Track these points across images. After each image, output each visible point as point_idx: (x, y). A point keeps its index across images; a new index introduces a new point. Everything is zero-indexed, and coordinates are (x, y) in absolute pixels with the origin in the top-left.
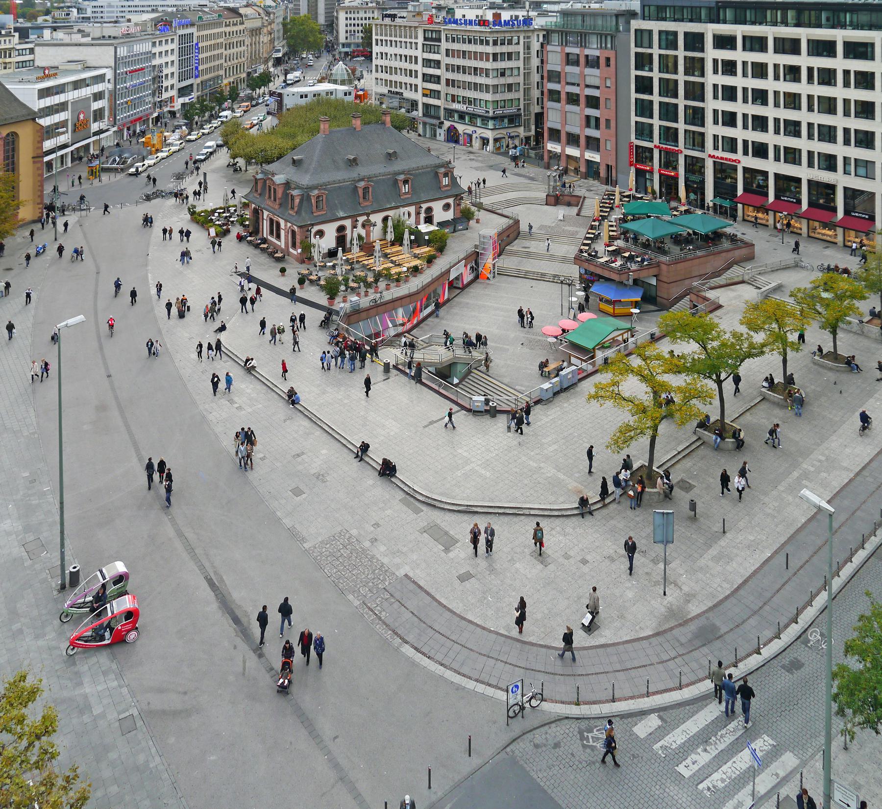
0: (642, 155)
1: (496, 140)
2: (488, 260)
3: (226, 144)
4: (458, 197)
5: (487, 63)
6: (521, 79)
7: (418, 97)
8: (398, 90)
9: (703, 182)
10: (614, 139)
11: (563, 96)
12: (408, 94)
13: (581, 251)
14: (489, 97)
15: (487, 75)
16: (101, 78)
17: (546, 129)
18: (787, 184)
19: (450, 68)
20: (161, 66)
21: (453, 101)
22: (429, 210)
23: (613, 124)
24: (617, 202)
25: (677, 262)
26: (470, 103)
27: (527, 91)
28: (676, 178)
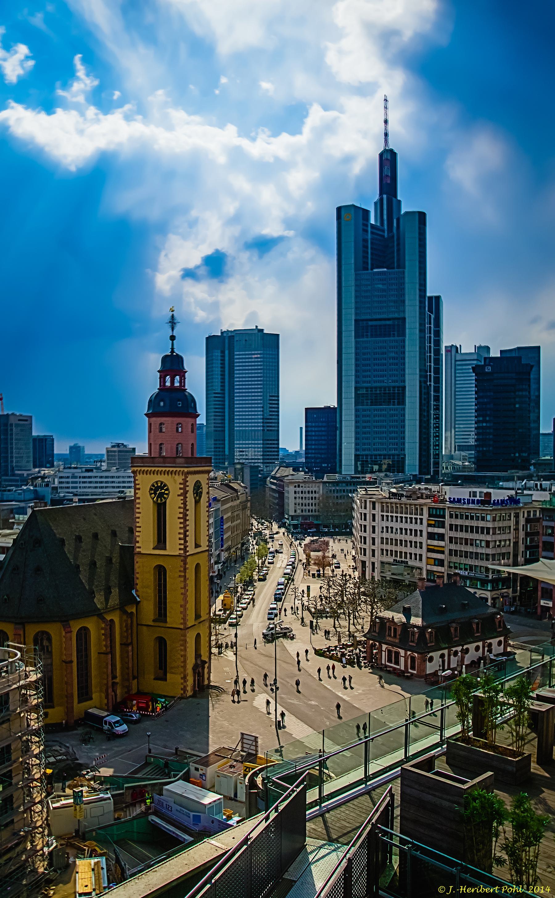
1: (493, 599)
5: (488, 536)
7: (423, 564)
8: (403, 559)
17: (540, 589)
21: (456, 568)
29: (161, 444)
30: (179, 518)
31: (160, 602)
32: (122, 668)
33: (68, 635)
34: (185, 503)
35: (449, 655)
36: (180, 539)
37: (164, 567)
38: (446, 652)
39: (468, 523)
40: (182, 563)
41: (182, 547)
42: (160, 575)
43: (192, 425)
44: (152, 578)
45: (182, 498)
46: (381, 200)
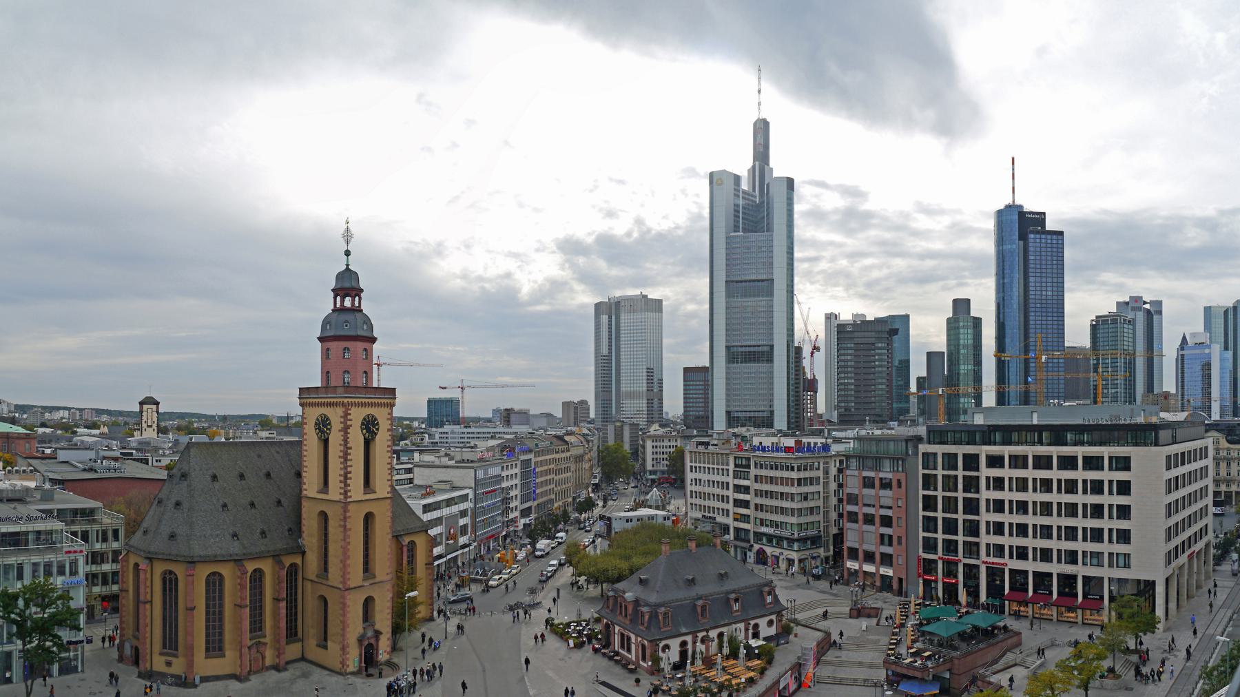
0: (929, 566)
2: (810, 669)
3: (569, 562)
4: (779, 614)
6: (820, 503)
7: (729, 521)
9: (978, 586)
11: (861, 517)
13: (888, 655)
14: (794, 520)
15: (792, 500)
16: (464, 498)
17: (845, 547)
18: (1042, 579)
19: (759, 493)
20: (507, 488)
21: (762, 525)
22: (756, 626)
23: (904, 540)
24: (912, 610)
25: (968, 654)
26: (777, 526)
27: (826, 513)
28: (956, 584)
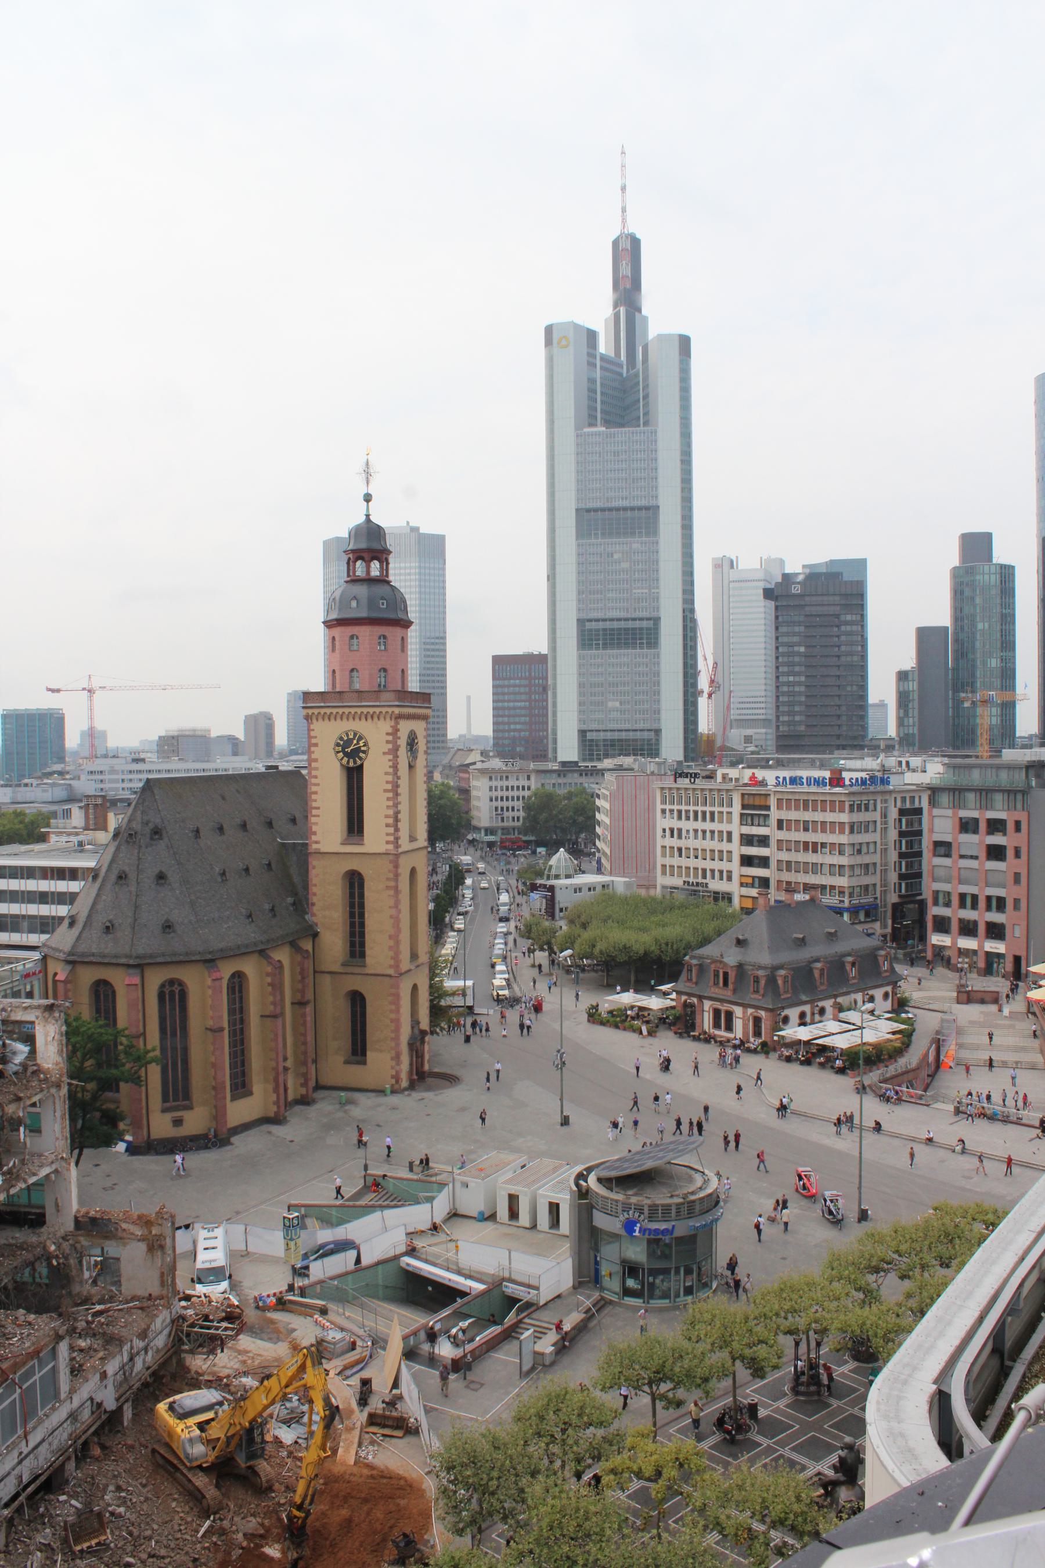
5: (842, 836)
10: (1025, 923)
12: (716, 885)
23: (1023, 905)
29: (352, 670)
30: (385, 791)
31: (352, 934)
32: (295, 1045)
33: (217, 983)
34: (395, 767)
35: (813, 1014)
36: (387, 825)
37: (360, 874)
38: (807, 1008)
39: (808, 816)
40: (391, 866)
41: (391, 838)
42: (352, 886)
43: (403, 638)
44: (339, 892)
45: (391, 757)
46: (617, 316)
